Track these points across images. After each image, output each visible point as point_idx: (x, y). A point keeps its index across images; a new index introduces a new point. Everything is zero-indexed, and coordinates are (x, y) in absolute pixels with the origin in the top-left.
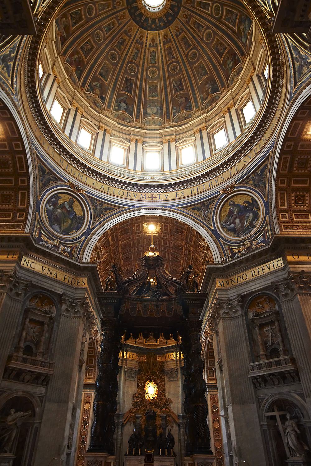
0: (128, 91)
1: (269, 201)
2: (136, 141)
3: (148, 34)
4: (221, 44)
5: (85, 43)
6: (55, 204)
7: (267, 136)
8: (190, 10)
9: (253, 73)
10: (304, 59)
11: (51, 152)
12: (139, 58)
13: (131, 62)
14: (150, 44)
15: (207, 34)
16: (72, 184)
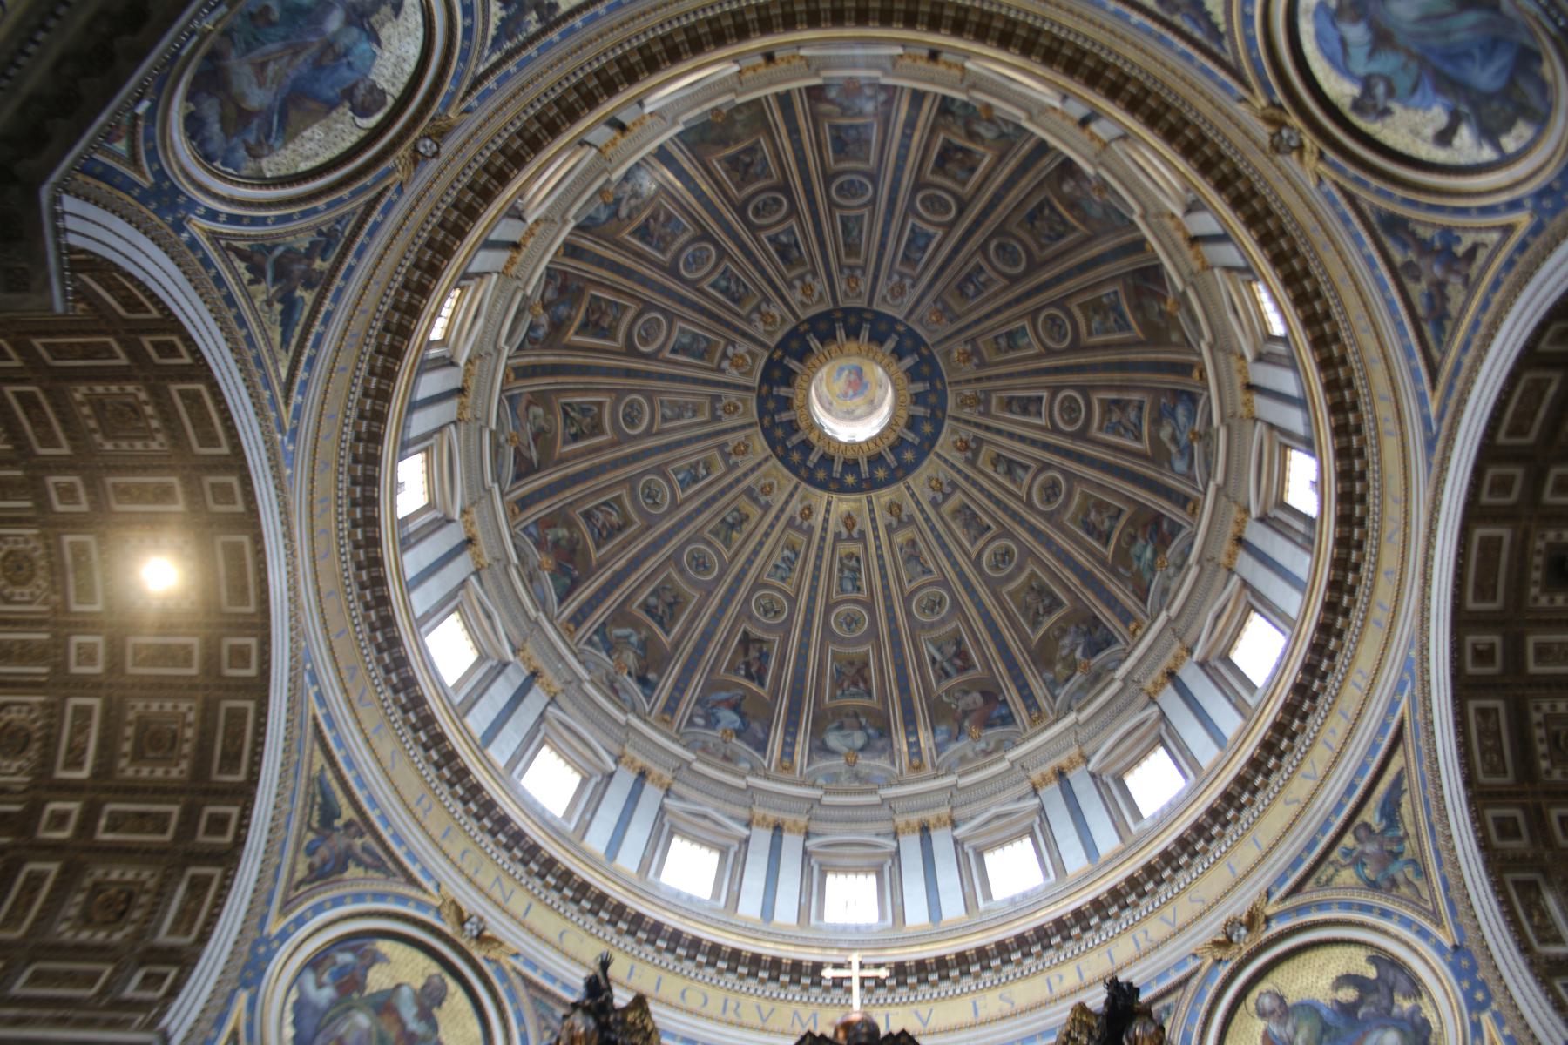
0: (749, 676)
1: (1470, 933)
2: (778, 829)
3: (829, 503)
4: (1101, 506)
5: (605, 503)
6: (350, 983)
7: (1366, 658)
8: (978, 425)
9: (1241, 524)
10: (1439, 252)
11: (386, 747)
12: (796, 574)
13: (766, 586)
14: (837, 536)
15: (1043, 488)
16: (453, 902)
